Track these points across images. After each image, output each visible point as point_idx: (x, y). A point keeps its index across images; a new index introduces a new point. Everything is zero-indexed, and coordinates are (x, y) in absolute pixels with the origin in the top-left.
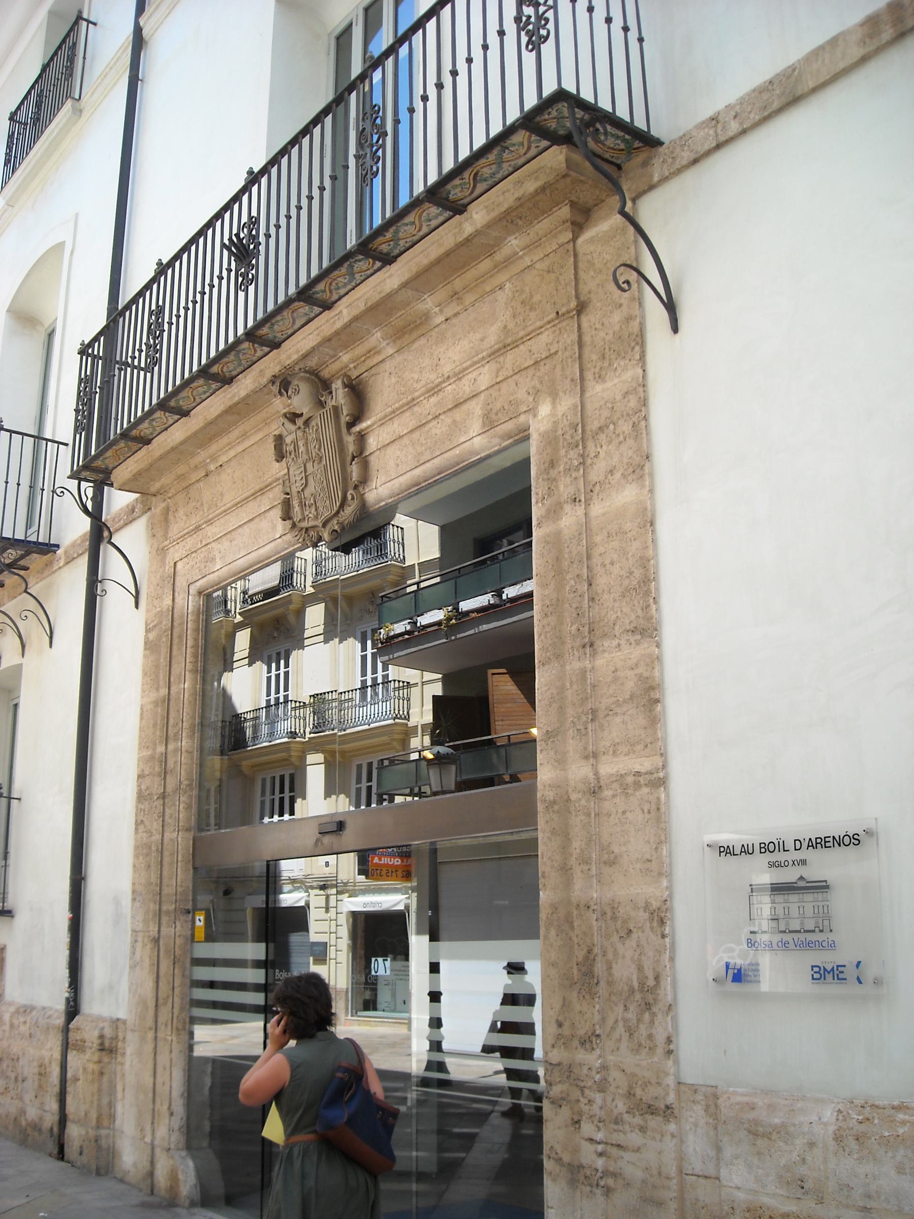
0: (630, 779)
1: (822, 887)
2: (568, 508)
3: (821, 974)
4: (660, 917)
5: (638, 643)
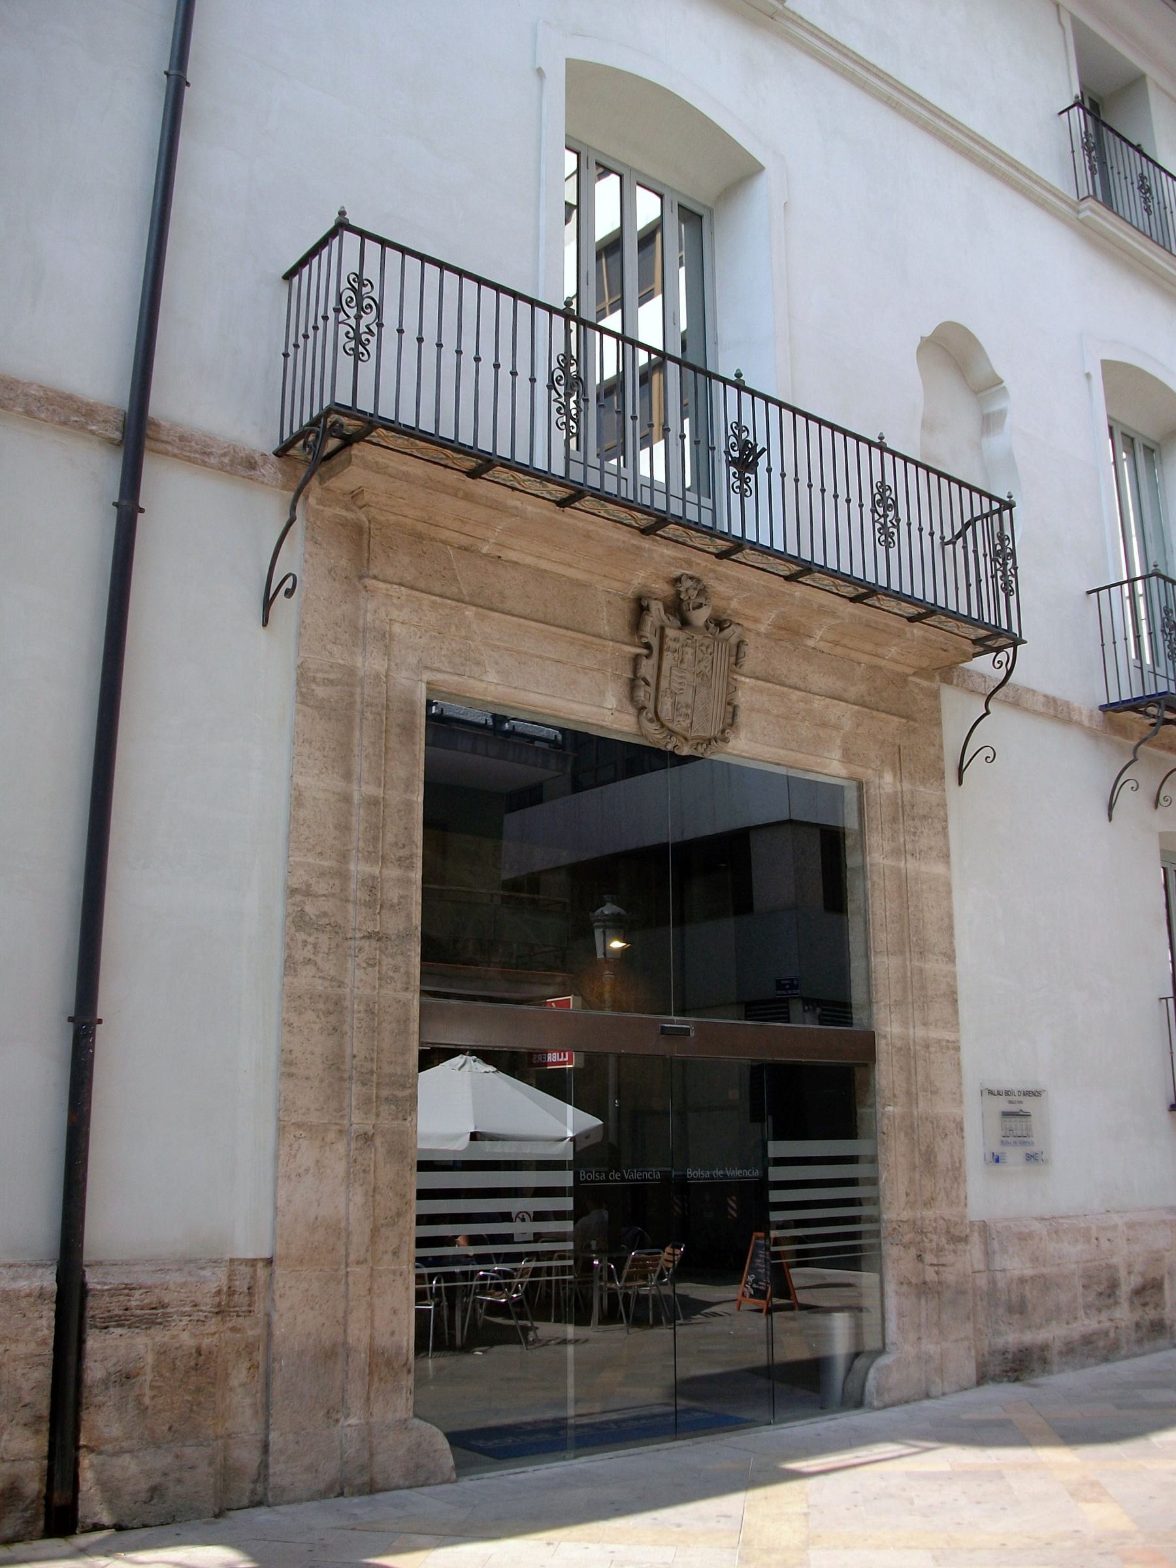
1: (1027, 1115)
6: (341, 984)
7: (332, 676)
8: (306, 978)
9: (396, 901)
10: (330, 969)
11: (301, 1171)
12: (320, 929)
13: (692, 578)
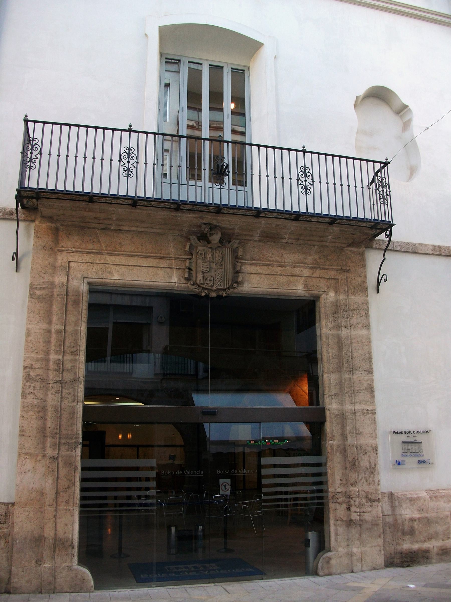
0: (365, 411)
1: (420, 442)
2: (343, 329)
3: (420, 462)
4: (375, 449)
5: (368, 374)
6: (45, 401)
7: (44, 286)
8: (30, 399)
9: (69, 368)
10: (40, 395)
11: (27, 471)
12: (36, 381)
13: (205, 224)
